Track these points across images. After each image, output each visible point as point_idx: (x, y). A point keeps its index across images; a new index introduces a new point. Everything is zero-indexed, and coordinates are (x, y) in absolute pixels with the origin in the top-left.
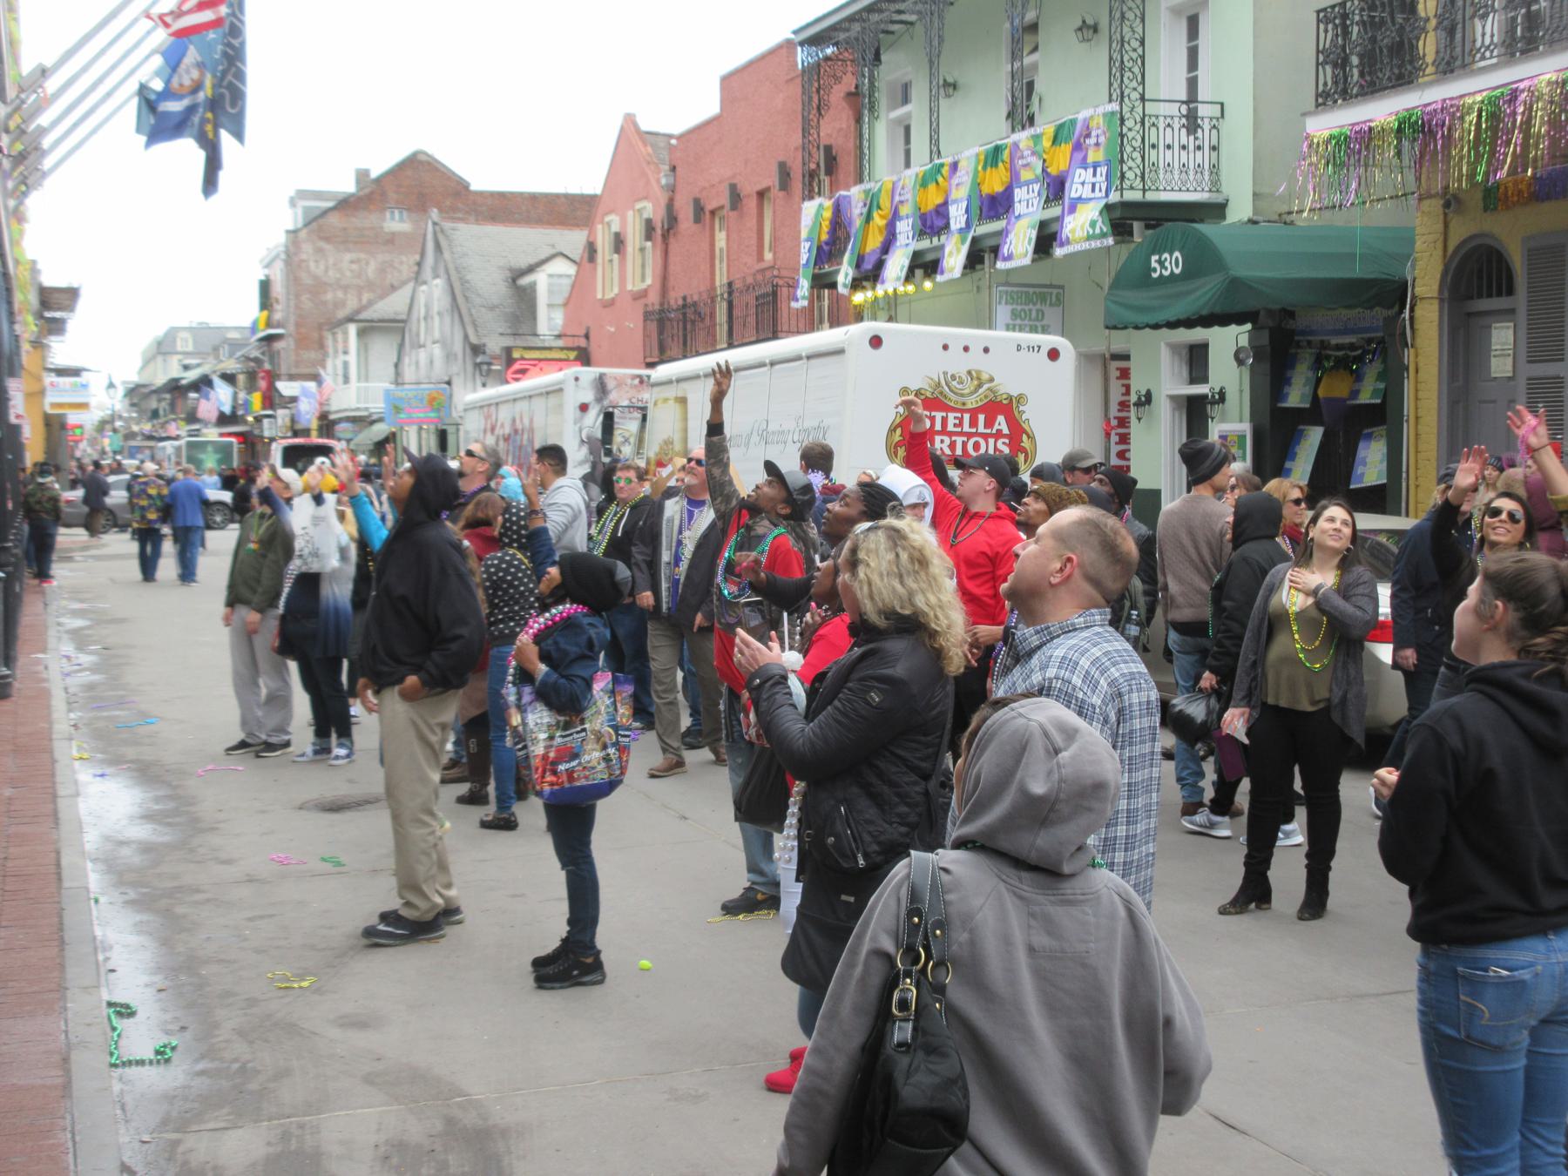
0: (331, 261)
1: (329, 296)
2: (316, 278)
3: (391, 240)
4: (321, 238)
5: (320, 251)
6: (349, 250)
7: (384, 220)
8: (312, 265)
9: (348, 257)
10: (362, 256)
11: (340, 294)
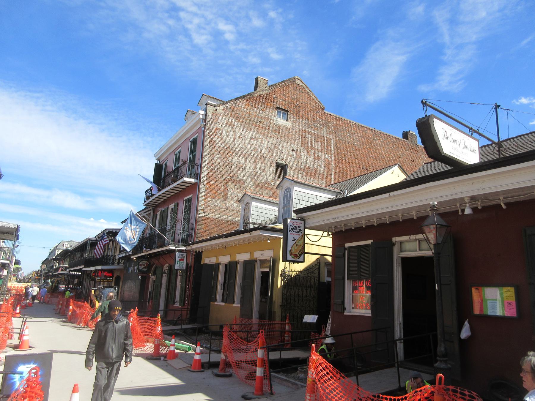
0: (238, 135)
1: (235, 160)
2: (226, 144)
3: (278, 129)
4: (231, 116)
5: (230, 125)
6: (249, 129)
7: (274, 116)
8: (224, 133)
9: (249, 134)
10: (259, 136)
11: (242, 160)
